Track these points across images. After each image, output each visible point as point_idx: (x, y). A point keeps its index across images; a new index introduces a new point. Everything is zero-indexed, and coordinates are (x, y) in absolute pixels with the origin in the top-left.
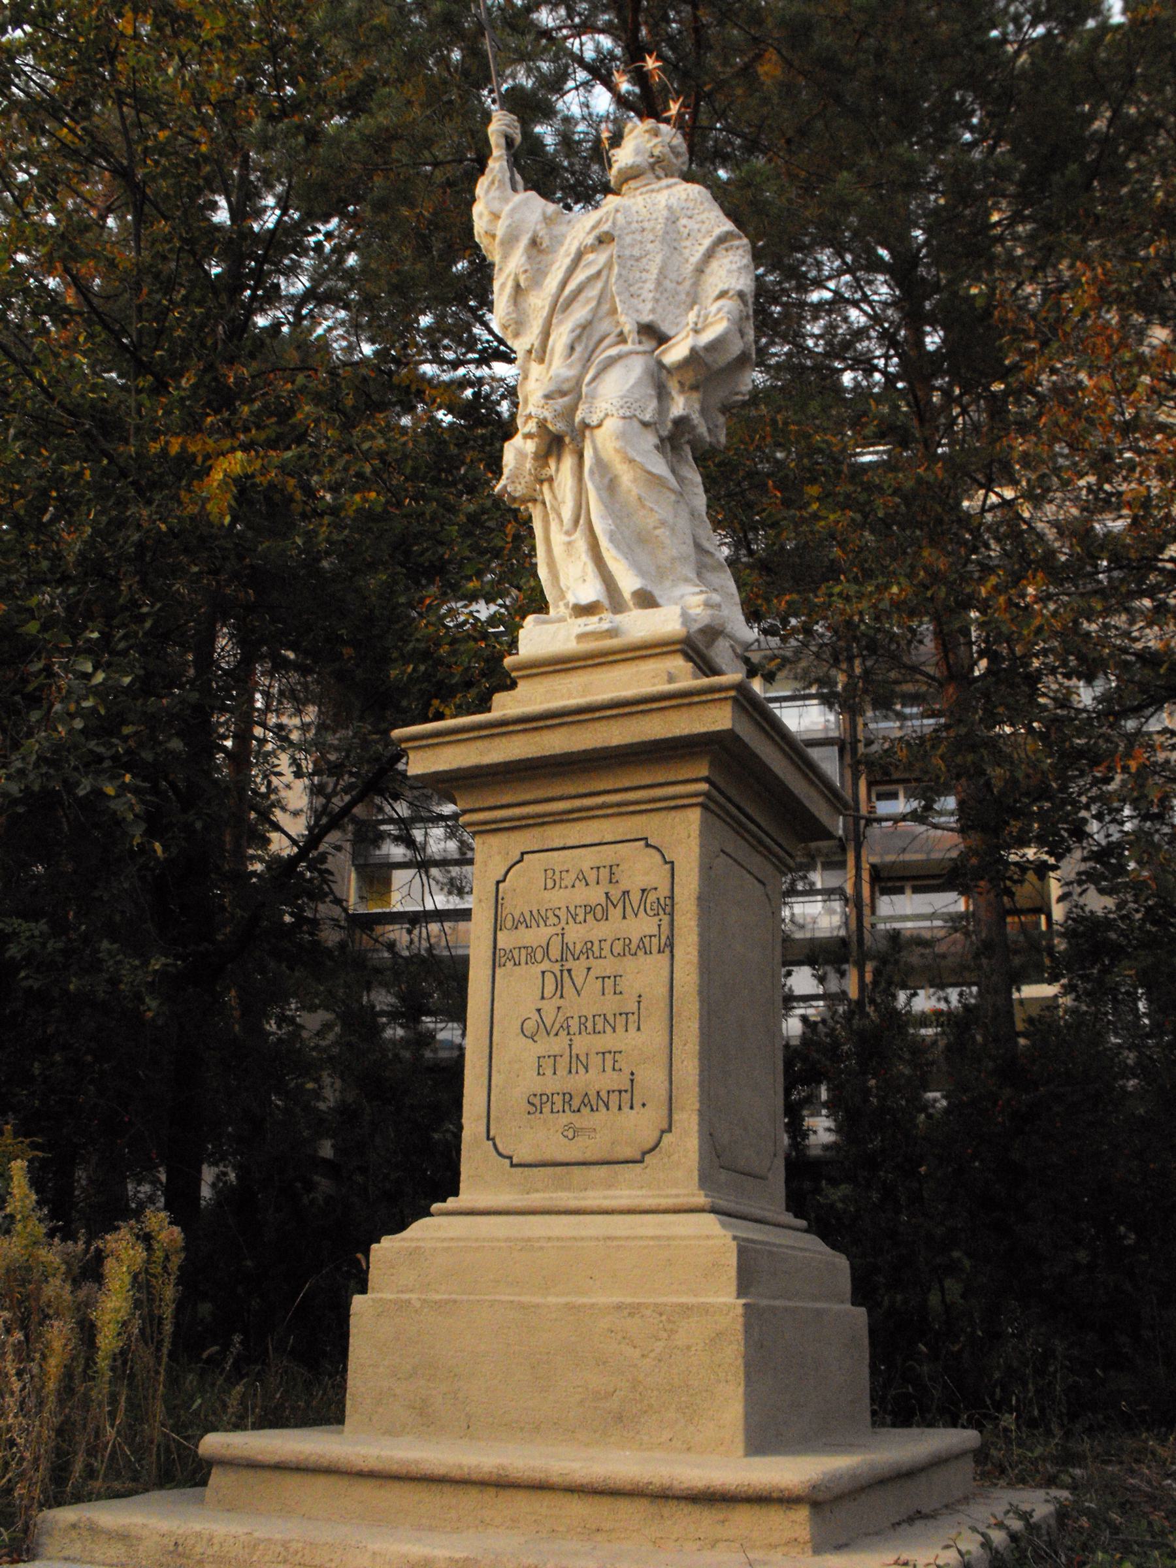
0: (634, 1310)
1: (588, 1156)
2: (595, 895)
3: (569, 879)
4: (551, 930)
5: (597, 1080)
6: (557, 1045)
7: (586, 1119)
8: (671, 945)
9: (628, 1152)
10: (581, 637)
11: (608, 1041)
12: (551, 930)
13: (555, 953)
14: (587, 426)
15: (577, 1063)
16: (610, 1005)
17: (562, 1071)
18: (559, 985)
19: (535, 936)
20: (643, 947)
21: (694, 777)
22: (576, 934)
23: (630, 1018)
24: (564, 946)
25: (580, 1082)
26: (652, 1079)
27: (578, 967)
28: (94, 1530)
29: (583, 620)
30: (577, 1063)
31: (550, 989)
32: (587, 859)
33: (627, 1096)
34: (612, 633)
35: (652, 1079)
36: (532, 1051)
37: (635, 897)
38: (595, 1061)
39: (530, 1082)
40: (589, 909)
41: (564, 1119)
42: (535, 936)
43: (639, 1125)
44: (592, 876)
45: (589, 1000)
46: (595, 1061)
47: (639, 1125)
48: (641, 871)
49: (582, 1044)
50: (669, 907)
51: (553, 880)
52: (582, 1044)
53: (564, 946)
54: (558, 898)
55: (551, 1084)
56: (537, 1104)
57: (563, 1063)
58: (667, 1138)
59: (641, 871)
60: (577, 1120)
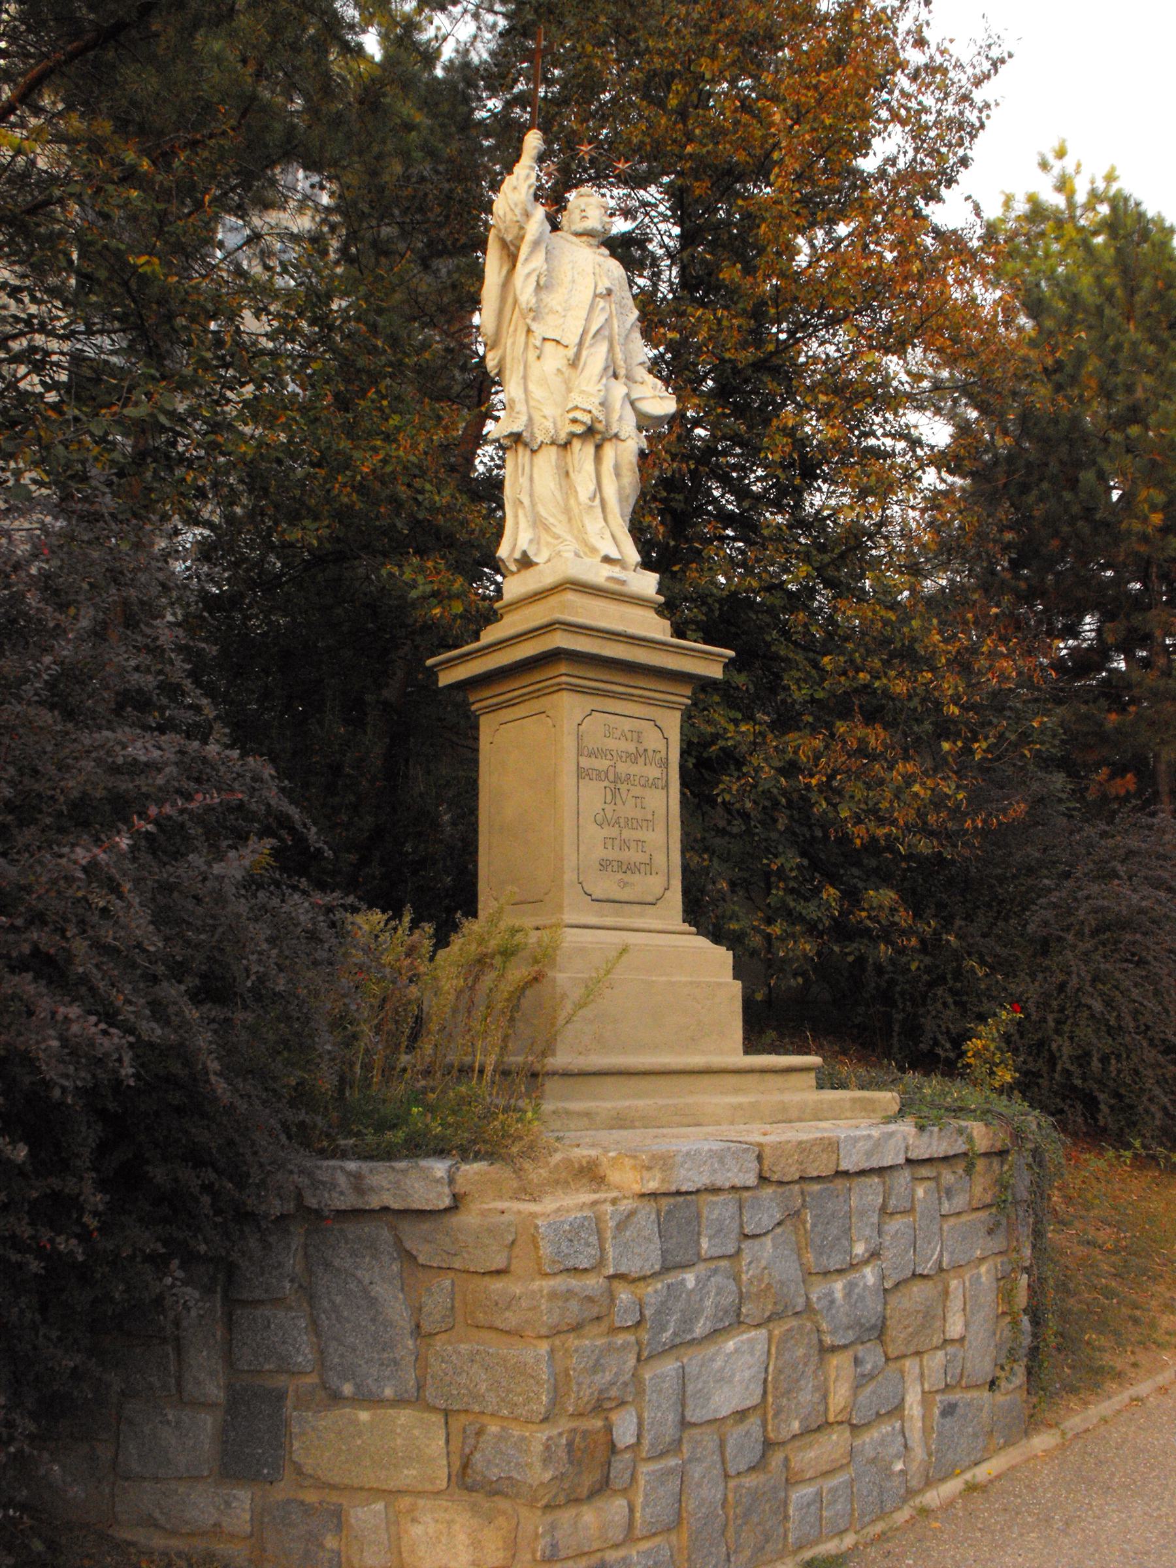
0: (698, 984)
1: (632, 898)
2: (631, 747)
3: (618, 734)
4: (608, 763)
5: (634, 856)
6: (614, 832)
7: (629, 878)
8: (667, 785)
9: (651, 899)
10: (609, 579)
11: (639, 834)
12: (608, 763)
13: (611, 777)
14: (616, 436)
15: (625, 844)
16: (639, 814)
17: (617, 848)
18: (614, 796)
19: (603, 764)
20: (654, 785)
21: (683, 695)
22: (623, 768)
23: (648, 823)
24: (616, 774)
25: (625, 855)
26: (660, 859)
27: (623, 787)
28: (568, 1113)
29: (606, 566)
30: (625, 844)
31: (609, 798)
32: (627, 725)
33: (648, 867)
34: (623, 583)
35: (660, 859)
36: (607, 831)
37: (650, 753)
38: (633, 845)
39: (600, 853)
40: (629, 755)
41: (620, 876)
42: (603, 764)
43: (653, 884)
44: (629, 735)
45: (628, 810)
46: (633, 845)
47: (653, 884)
48: (653, 741)
49: (626, 833)
50: (665, 763)
51: (609, 733)
52: (626, 833)
53: (616, 774)
54: (611, 744)
55: (612, 854)
56: (604, 865)
57: (617, 842)
58: (668, 894)
59: (653, 741)
60: (626, 878)
